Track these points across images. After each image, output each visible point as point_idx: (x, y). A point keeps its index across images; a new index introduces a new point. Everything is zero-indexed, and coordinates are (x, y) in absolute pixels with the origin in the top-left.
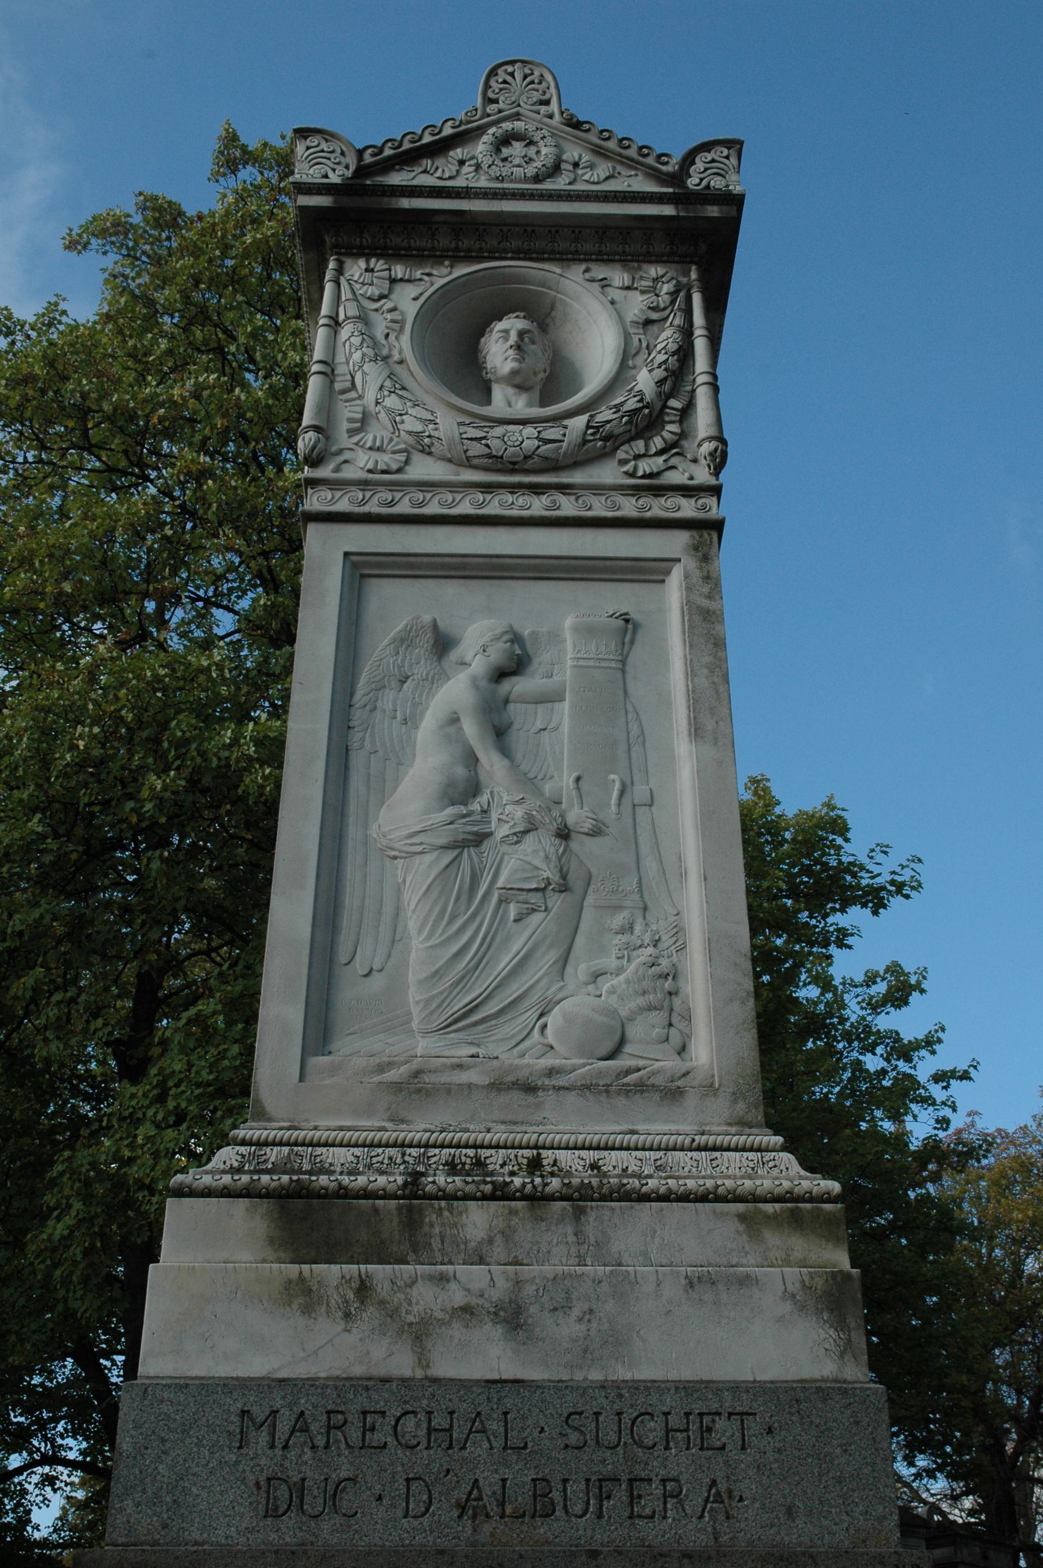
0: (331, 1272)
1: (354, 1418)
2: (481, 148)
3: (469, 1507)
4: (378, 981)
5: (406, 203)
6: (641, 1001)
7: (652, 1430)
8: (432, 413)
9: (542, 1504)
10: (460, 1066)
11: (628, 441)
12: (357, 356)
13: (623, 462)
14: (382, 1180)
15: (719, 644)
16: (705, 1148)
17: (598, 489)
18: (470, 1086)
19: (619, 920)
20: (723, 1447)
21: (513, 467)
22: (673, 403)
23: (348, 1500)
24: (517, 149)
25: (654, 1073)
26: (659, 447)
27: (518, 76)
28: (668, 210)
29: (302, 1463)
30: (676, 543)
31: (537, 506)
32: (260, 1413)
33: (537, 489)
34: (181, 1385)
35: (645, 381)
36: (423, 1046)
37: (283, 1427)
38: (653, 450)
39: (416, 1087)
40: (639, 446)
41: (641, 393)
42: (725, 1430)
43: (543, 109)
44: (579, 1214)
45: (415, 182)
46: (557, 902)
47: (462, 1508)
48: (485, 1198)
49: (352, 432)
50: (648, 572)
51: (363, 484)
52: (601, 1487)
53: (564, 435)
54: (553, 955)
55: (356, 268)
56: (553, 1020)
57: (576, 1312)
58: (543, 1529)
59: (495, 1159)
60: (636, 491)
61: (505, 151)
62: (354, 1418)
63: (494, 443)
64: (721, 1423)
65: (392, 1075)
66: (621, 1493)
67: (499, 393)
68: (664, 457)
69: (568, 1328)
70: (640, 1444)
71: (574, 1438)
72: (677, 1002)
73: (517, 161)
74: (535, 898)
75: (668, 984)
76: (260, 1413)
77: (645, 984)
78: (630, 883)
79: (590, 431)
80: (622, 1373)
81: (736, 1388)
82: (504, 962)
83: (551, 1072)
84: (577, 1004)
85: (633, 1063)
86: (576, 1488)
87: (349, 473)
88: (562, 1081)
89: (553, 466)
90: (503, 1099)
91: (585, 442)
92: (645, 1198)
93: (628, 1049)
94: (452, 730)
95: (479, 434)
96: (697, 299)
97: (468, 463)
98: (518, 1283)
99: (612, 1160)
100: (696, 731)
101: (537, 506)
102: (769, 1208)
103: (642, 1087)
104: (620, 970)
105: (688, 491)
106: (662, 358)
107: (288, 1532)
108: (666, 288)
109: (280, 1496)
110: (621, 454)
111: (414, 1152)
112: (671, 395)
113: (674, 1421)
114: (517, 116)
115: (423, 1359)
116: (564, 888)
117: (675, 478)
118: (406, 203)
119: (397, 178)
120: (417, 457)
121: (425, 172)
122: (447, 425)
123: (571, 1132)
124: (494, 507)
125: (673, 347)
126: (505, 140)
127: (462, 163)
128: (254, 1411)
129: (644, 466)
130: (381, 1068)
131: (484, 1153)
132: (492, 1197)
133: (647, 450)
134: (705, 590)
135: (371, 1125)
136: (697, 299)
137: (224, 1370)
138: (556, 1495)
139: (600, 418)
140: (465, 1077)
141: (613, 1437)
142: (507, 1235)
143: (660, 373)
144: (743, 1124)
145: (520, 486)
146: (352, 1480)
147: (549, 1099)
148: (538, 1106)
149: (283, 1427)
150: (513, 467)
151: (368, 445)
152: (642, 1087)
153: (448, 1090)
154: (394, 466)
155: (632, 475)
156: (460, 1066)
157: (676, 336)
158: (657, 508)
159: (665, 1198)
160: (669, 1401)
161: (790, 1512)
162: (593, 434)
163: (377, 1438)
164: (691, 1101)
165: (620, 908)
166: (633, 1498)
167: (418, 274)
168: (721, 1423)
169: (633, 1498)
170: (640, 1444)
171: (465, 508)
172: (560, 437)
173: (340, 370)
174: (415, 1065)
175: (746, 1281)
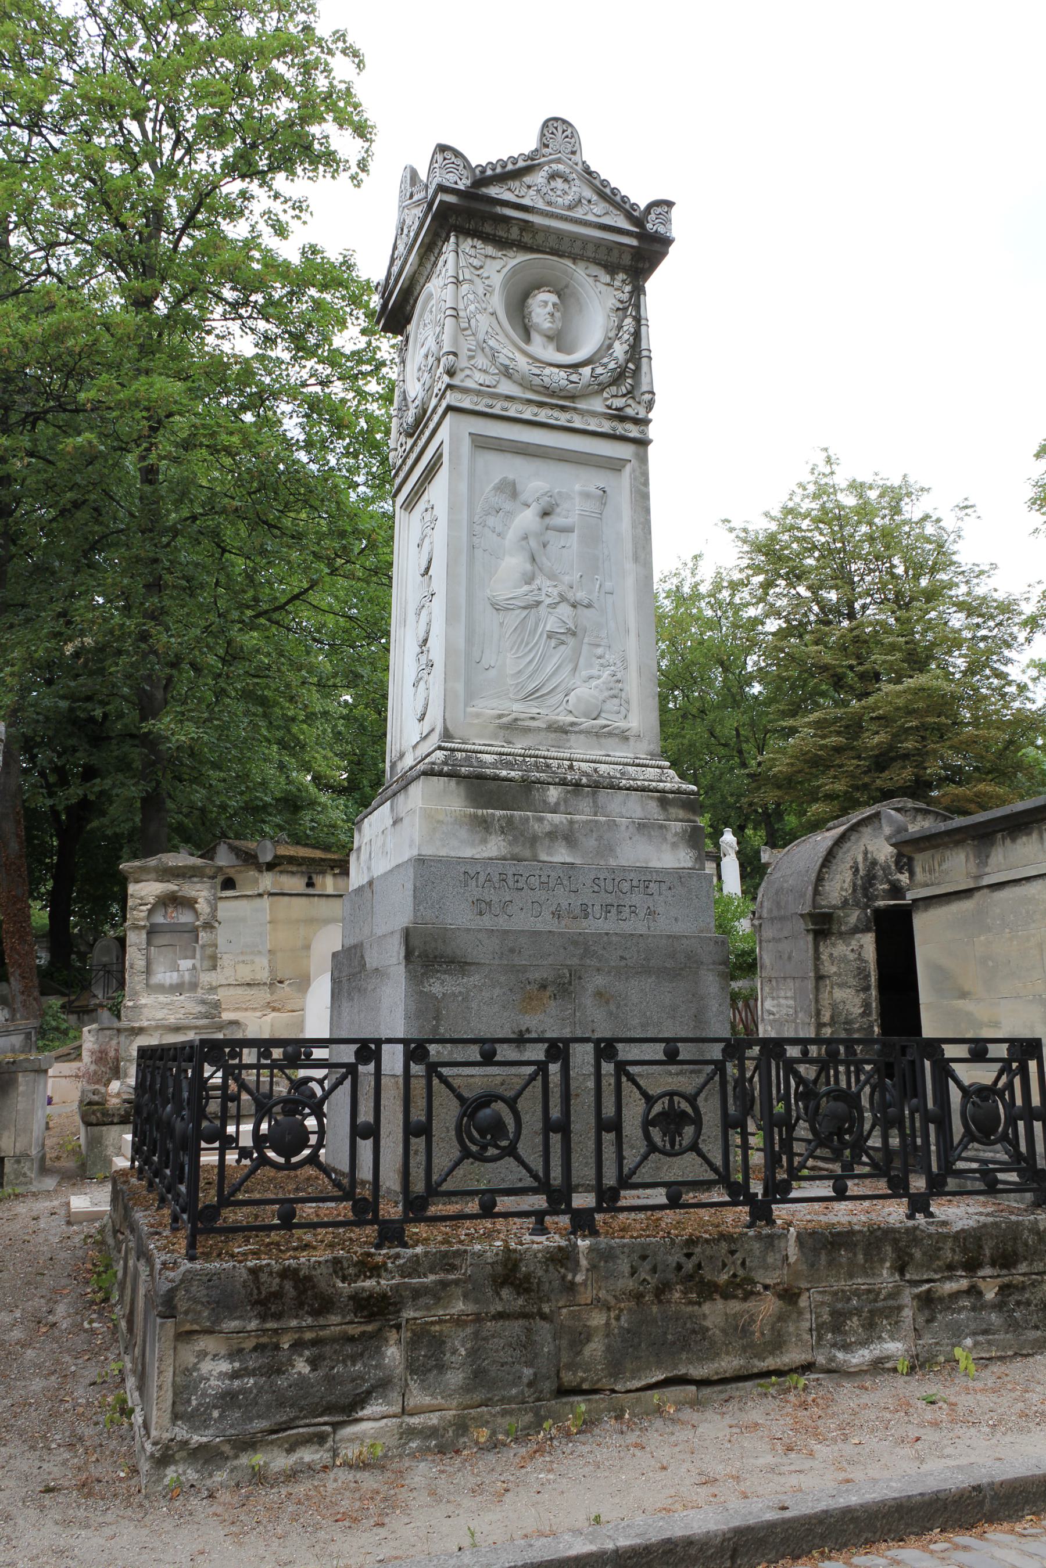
1: (510, 876)
2: (539, 178)
3: (557, 914)
4: (492, 673)
5: (499, 210)
7: (626, 886)
10: (533, 718)
12: (472, 307)
15: (647, 511)
16: (638, 765)
19: (599, 651)
21: (553, 394)
23: (510, 910)
24: (559, 183)
28: (634, 242)
29: (490, 895)
32: (472, 873)
33: (563, 408)
35: (620, 350)
36: (517, 707)
37: (482, 878)
40: (613, 389)
41: (616, 359)
44: (594, 793)
46: (571, 641)
51: (478, 393)
52: (607, 908)
54: (570, 667)
55: (467, 244)
56: (572, 697)
58: (585, 923)
59: (554, 763)
61: (553, 184)
62: (510, 876)
63: (545, 379)
64: (652, 885)
65: (504, 720)
66: (614, 910)
67: (536, 338)
69: (591, 843)
71: (596, 888)
72: (623, 694)
73: (559, 193)
74: (563, 637)
76: (472, 873)
77: (612, 685)
80: (613, 862)
81: (657, 871)
82: (549, 669)
83: (573, 724)
86: (597, 908)
87: (470, 384)
88: (577, 729)
89: (573, 398)
92: (620, 788)
93: (603, 715)
94: (524, 543)
97: (531, 388)
98: (571, 822)
100: (636, 559)
102: (670, 796)
103: (610, 734)
104: (599, 677)
106: (626, 336)
107: (487, 921)
108: (628, 288)
109: (482, 906)
110: (605, 395)
113: (635, 883)
114: (558, 161)
117: (630, 412)
118: (499, 210)
120: (503, 379)
123: (584, 755)
126: (553, 176)
127: (529, 187)
130: (500, 716)
132: (559, 784)
137: (453, 854)
142: (565, 801)
144: (653, 755)
145: (557, 406)
147: (573, 737)
148: (568, 740)
149: (482, 878)
150: (553, 394)
152: (610, 734)
155: (609, 407)
156: (533, 718)
158: (620, 429)
159: (628, 789)
160: (632, 875)
161: (676, 919)
165: (599, 646)
168: (652, 885)
173: (462, 314)
174: (514, 716)
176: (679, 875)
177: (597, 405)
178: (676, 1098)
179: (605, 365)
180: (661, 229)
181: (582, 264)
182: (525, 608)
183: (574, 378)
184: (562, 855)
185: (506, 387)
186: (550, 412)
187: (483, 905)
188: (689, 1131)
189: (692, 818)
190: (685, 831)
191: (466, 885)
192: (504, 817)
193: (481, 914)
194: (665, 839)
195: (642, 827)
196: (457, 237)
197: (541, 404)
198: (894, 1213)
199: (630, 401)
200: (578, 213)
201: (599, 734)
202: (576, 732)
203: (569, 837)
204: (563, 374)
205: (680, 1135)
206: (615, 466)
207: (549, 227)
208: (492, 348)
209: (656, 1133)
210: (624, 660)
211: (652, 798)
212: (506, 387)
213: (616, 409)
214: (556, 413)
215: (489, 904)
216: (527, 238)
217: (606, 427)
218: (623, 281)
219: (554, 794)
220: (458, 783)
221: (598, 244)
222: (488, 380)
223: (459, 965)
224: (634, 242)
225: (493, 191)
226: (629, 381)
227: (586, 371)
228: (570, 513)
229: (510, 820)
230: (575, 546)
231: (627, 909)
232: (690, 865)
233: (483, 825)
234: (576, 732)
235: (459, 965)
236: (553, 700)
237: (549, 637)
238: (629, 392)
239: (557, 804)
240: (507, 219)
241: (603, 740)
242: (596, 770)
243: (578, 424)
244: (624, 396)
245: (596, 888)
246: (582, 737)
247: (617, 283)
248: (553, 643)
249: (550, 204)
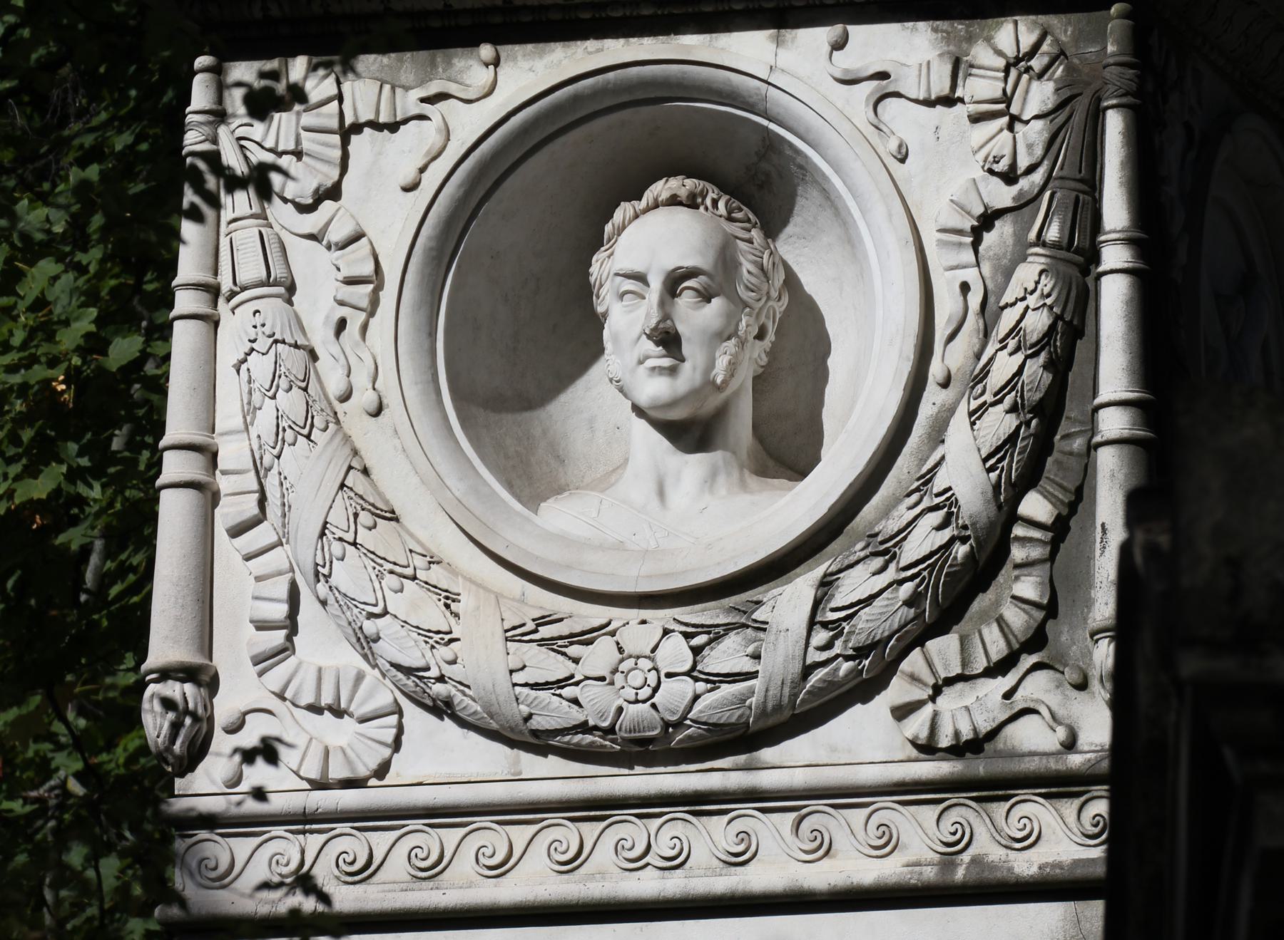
8: (449, 600)
11: (920, 641)
13: (902, 712)
22: (1035, 506)
26: (995, 657)
38: (980, 664)
40: (944, 649)
53: (756, 657)
68: (1004, 683)
79: (821, 636)
91: (807, 670)
95: (556, 667)
96: (1114, 124)
106: (1004, 366)
108: (1040, 95)
112: (1029, 479)
117: (1033, 737)
125: (1037, 323)
129: (964, 711)
133: (965, 663)
136: (1114, 124)
143: (999, 423)
151: (307, 698)
155: (927, 749)
157: (1047, 284)
162: (828, 646)
167: (410, 102)
172: (747, 665)
177: (864, 740)
179: (886, 551)
185: (445, 759)
186: (633, 831)
199: (1038, 687)
212: (445, 759)
213: (959, 750)
214: (669, 833)
217: (918, 840)
218: (1016, 63)
222: (352, 744)
227: (789, 602)
238: (1037, 640)
243: (778, 864)
247: (981, 88)
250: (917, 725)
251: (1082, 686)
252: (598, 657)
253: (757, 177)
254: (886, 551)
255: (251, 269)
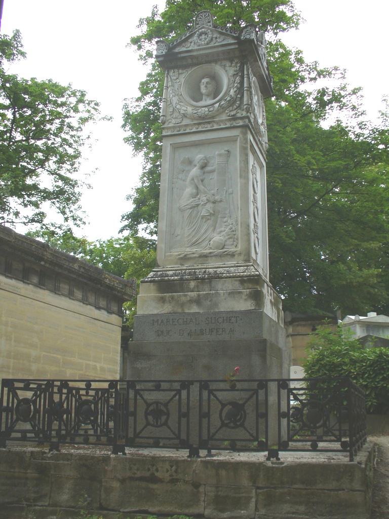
0: (167, 295)
4: (179, 238)
6: (229, 236)
7: (221, 320)
9: (202, 332)
10: (193, 253)
12: (171, 96)
14: (176, 277)
17: (222, 121)
18: (195, 257)
19: (225, 219)
20: (233, 323)
24: (203, 36)
25: (231, 251)
27: (203, 16)
28: (237, 46)
30: (236, 132)
31: (209, 127)
33: (209, 123)
34: (143, 316)
37: (160, 322)
39: (185, 259)
40: (231, 108)
42: (233, 320)
43: (209, 24)
44: (210, 282)
45: (181, 50)
46: (212, 218)
47: (188, 334)
48: (194, 280)
49: (171, 115)
50: (233, 140)
52: (211, 331)
54: (212, 229)
56: (211, 242)
57: (209, 300)
60: (230, 120)
61: (201, 37)
63: (199, 114)
64: (232, 318)
65: (181, 256)
70: (218, 322)
71: (207, 322)
72: (235, 236)
73: (203, 40)
74: (209, 217)
75: (234, 233)
77: (229, 233)
78: (227, 212)
81: (236, 312)
82: (203, 231)
83: (210, 253)
84: (217, 238)
85: (226, 250)
86: (208, 330)
88: (212, 255)
90: (200, 259)
93: (225, 247)
94: (192, 182)
95: (196, 112)
98: (199, 295)
99: (219, 270)
100: (241, 177)
101: (209, 127)
102: (245, 278)
105: (242, 118)
106: (236, 85)
108: (239, 65)
110: (226, 111)
111: (183, 271)
114: (203, 28)
115: (183, 310)
116: (214, 215)
117: (239, 115)
119: (177, 50)
120: (184, 119)
121: (183, 46)
122: (190, 110)
124: (200, 129)
125: (239, 81)
126: (201, 34)
127: (191, 42)
128: (154, 319)
129: (232, 113)
130: (179, 255)
131: (196, 270)
134: (244, 142)
135: (177, 267)
137: (151, 313)
138: (204, 332)
139: (222, 103)
140: (194, 255)
141: (214, 321)
142: (198, 286)
143: (235, 89)
145: (206, 122)
146: (171, 330)
147: (209, 258)
149: (160, 322)
150: (203, 118)
153: (191, 258)
154: (180, 121)
155: (229, 116)
156: (193, 253)
161: (244, 333)
163: (175, 323)
164: (236, 256)
165: (225, 217)
166: (217, 332)
169: (217, 332)
170: (218, 322)
171: (194, 130)
173: (168, 100)
175: (240, 293)
176: (247, 313)
177: (224, 117)
178: (159, 405)
180: (248, 37)
181: (219, 63)
182: (191, 208)
183: (211, 109)
184: (195, 309)
186: (203, 126)
187: (160, 332)
188: (164, 418)
189: (256, 287)
190: (250, 293)
191: (153, 325)
192: (170, 296)
193: (159, 336)
194: (241, 298)
195: (233, 294)
196: (168, 71)
197: (199, 124)
198: (260, 457)
199: (239, 111)
200: (212, 44)
201: (221, 256)
202: (211, 256)
203: (198, 301)
204: (207, 109)
205: (160, 419)
206: (233, 140)
207: (200, 54)
208: (178, 109)
209: (150, 418)
210: (237, 221)
211: (236, 280)
212: (186, 122)
213: (232, 116)
215: (162, 332)
216: (195, 61)
217: (228, 125)
219: (192, 284)
220: (154, 284)
221: (223, 52)
222: (179, 121)
223: (148, 356)
224: (237, 46)
225: (177, 50)
226: (238, 102)
228: (214, 164)
229: (173, 298)
230: (216, 178)
231: (221, 330)
232: (253, 308)
233: (162, 300)
234: (211, 256)
235: (148, 356)
236: (204, 244)
237: (202, 218)
238: (239, 107)
239: (194, 288)
240: (184, 58)
241: (223, 258)
242: (216, 272)
243: (216, 127)
244: (235, 109)
245: (207, 322)
246: (214, 258)
248: (204, 220)
249: (199, 46)
250: (228, 114)
251: (243, 110)
252: (200, 110)
253: (214, 78)
254: (226, 100)
255: (170, 84)
